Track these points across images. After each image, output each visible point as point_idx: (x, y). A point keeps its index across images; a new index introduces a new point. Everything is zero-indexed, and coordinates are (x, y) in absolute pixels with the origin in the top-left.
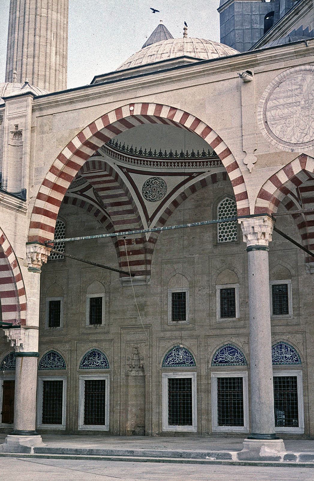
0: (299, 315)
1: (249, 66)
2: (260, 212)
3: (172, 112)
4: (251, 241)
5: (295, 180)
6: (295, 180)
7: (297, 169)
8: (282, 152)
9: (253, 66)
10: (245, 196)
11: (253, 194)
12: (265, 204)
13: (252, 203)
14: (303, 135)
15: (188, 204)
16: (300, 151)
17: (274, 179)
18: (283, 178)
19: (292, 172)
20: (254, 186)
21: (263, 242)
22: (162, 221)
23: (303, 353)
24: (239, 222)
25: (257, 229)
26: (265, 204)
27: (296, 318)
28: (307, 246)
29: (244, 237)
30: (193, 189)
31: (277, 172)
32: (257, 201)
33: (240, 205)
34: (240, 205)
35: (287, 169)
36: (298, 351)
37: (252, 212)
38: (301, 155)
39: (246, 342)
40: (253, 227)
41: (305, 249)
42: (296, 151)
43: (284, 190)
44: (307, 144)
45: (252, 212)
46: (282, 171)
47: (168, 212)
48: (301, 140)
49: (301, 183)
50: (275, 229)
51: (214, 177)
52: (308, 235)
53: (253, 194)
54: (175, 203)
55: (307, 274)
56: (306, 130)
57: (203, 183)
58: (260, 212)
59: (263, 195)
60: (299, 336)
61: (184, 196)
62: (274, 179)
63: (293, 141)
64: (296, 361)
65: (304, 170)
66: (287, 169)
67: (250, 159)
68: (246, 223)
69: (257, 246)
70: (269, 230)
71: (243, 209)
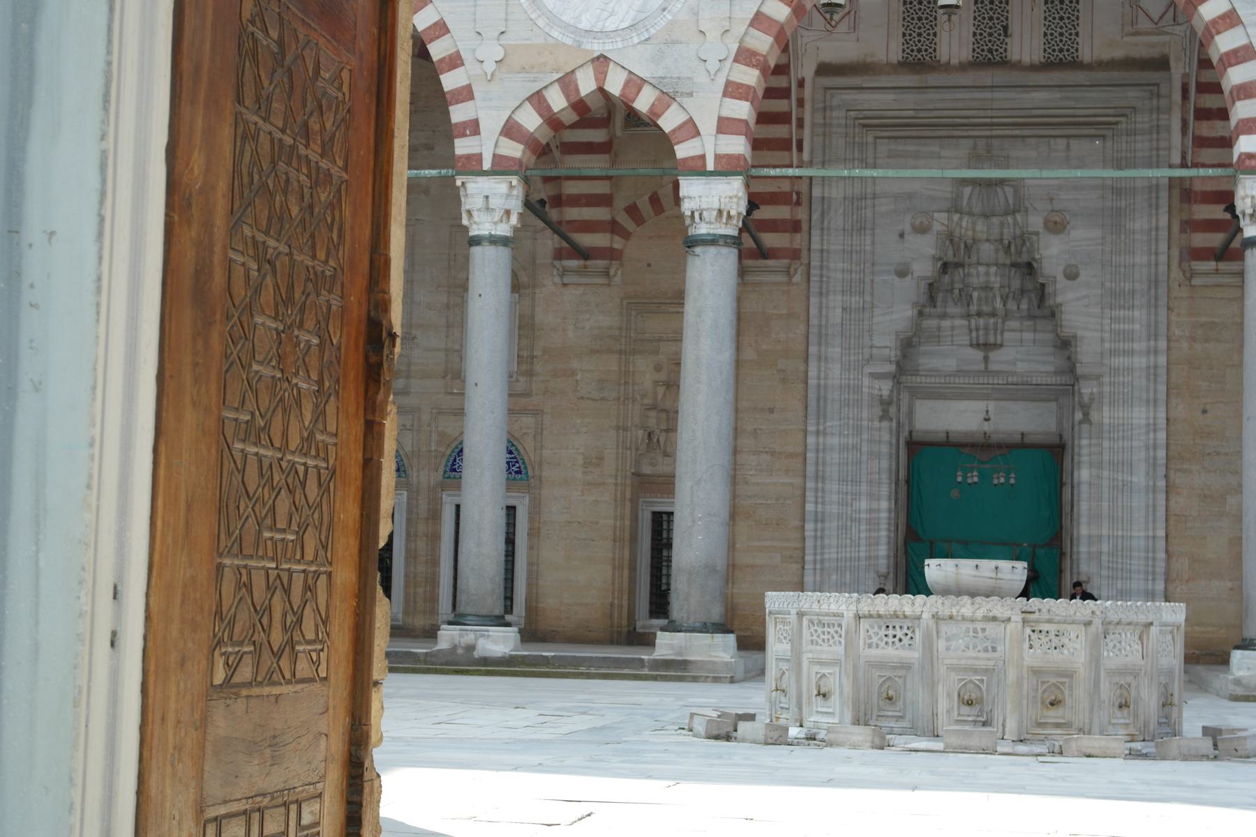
0: (530, 374)
2: (501, 167)
4: (482, 225)
5: (579, 106)
6: (579, 106)
7: (586, 85)
8: (559, 45)
10: (473, 127)
11: (491, 124)
12: (514, 150)
14: (606, 14)
16: (597, 48)
17: (537, 99)
18: (557, 101)
19: (577, 90)
20: (495, 109)
21: (504, 230)
23: (532, 455)
24: (459, 183)
25: (495, 202)
26: (514, 150)
27: (522, 379)
28: (560, 223)
29: (464, 216)
31: (545, 87)
32: (500, 143)
33: (463, 147)
34: (463, 147)
35: (567, 82)
36: (522, 452)
37: (487, 165)
38: (598, 58)
39: (408, 426)
40: (487, 197)
41: (555, 228)
42: (588, 47)
43: (553, 122)
44: (612, 35)
45: (487, 165)
46: (556, 86)
48: (598, 28)
49: (588, 109)
50: (527, 204)
52: (564, 198)
55: (555, 284)
56: (611, 5)
58: (501, 167)
59: (511, 130)
60: (528, 421)
62: (537, 99)
63: (584, 25)
64: (516, 472)
65: (601, 90)
66: (567, 82)
67: (491, 52)
69: (491, 236)
70: (516, 205)
71: (469, 157)
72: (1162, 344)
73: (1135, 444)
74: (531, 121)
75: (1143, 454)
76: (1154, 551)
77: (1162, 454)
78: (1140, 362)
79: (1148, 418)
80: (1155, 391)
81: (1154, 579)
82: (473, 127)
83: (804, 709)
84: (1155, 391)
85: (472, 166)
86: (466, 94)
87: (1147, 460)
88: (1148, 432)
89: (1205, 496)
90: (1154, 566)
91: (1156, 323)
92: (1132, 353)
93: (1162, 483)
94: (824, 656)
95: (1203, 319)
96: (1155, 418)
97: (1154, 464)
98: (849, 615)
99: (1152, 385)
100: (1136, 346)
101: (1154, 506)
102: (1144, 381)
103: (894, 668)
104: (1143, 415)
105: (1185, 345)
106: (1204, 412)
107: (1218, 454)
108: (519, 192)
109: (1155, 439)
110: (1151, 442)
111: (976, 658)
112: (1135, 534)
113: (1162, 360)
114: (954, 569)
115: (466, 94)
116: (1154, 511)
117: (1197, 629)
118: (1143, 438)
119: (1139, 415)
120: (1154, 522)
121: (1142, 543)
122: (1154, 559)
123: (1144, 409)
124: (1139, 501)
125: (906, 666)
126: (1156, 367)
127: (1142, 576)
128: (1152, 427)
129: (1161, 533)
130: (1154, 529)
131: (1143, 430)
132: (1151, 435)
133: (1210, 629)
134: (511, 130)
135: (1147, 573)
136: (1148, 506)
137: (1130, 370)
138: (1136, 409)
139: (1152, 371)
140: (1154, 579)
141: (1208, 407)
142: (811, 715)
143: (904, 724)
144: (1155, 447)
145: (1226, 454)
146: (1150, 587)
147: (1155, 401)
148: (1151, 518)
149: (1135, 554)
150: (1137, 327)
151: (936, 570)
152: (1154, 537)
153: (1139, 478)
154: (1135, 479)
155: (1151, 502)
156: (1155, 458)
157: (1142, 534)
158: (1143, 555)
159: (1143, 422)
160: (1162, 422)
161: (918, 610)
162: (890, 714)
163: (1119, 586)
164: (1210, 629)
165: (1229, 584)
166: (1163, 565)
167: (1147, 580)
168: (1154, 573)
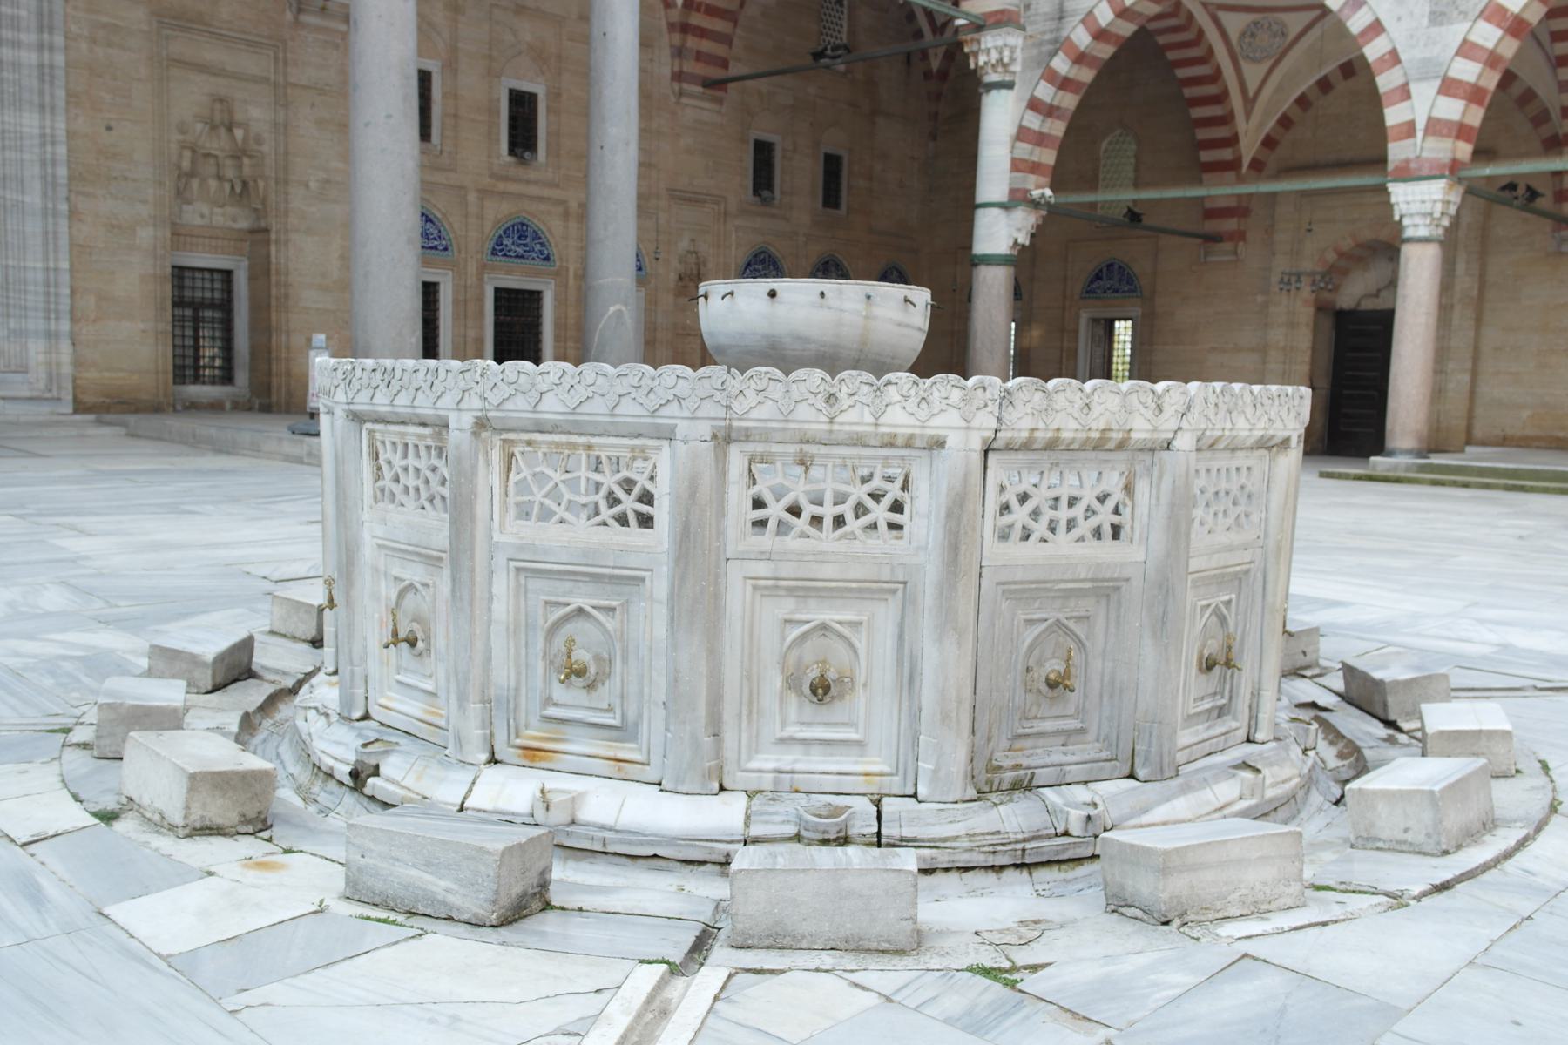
72: (59, 40)
73: (26, 156)
75: (37, 170)
76: (56, 286)
77: (62, 172)
78: (29, 57)
79: (43, 127)
80: (52, 96)
81: (57, 319)
83: (729, 736)
84: (52, 96)
87: (44, 178)
88: (43, 145)
89: (113, 226)
90: (57, 303)
91: (51, 13)
92: (16, 44)
93: (63, 207)
94: (828, 571)
95: (105, 19)
96: (53, 128)
97: (55, 185)
98: (963, 444)
99: (47, 87)
100: (23, 37)
101: (55, 233)
102: (35, 83)
103: (1068, 594)
104: (36, 123)
105: (84, 46)
106: (109, 128)
107: (126, 179)
109: (53, 154)
110: (48, 156)
111: (1230, 549)
112: (30, 264)
113: (60, 59)
114: (861, 306)
116: (56, 238)
117: (106, 374)
118: (37, 150)
119: (30, 122)
120: (56, 251)
121: (40, 276)
122: (57, 295)
123: (36, 116)
124: (33, 227)
125: (1106, 589)
126: (52, 67)
127: (41, 314)
128: (46, 139)
129: (65, 265)
130: (56, 260)
131: (37, 141)
132: (49, 148)
133: (121, 375)
135: (48, 311)
136: (47, 233)
137: (16, 66)
138: (26, 115)
139: (47, 70)
140: (57, 319)
141: (113, 124)
142: (755, 750)
143: (1087, 749)
144: (54, 163)
145: (134, 180)
146: (53, 327)
147: (53, 108)
148: (51, 247)
149: (31, 288)
150: (23, 13)
151: (733, 307)
152: (56, 269)
153: (33, 198)
154: (27, 199)
155: (50, 228)
156: (54, 176)
157: (39, 265)
158: (41, 289)
159: (36, 131)
160: (61, 134)
161: (1168, 423)
162: (1048, 726)
163: (12, 325)
164: (121, 375)
165: (141, 326)
166: (67, 301)
167: (48, 318)
168: (57, 311)
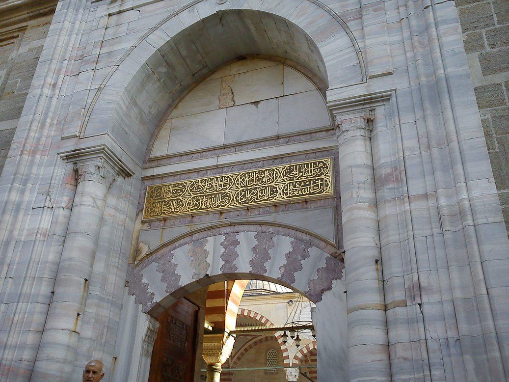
1: (291, 298)
2: (294, 366)
3: (256, 315)
9: (293, 298)
10: (288, 357)
11: (292, 357)
12: (297, 362)
13: (291, 361)
15: (252, 352)
22: (239, 359)
26: (297, 362)
28: (311, 377)
30: (256, 343)
34: (286, 361)
43: (305, 356)
47: (242, 354)
51: (266, 338)
53: (292, 357)
54: (246, 350)
57: (261, 340)
58: (294, 366)
59: (296, 358)
61: (250, 347)
68: (288, 370)
70: (297, 374)
74: (300, 355)
82: (288, 357)
85: (288, 366)
86: (286, 350)
108: (298, 371)
115: (286, 350)
134: (296, 358)
